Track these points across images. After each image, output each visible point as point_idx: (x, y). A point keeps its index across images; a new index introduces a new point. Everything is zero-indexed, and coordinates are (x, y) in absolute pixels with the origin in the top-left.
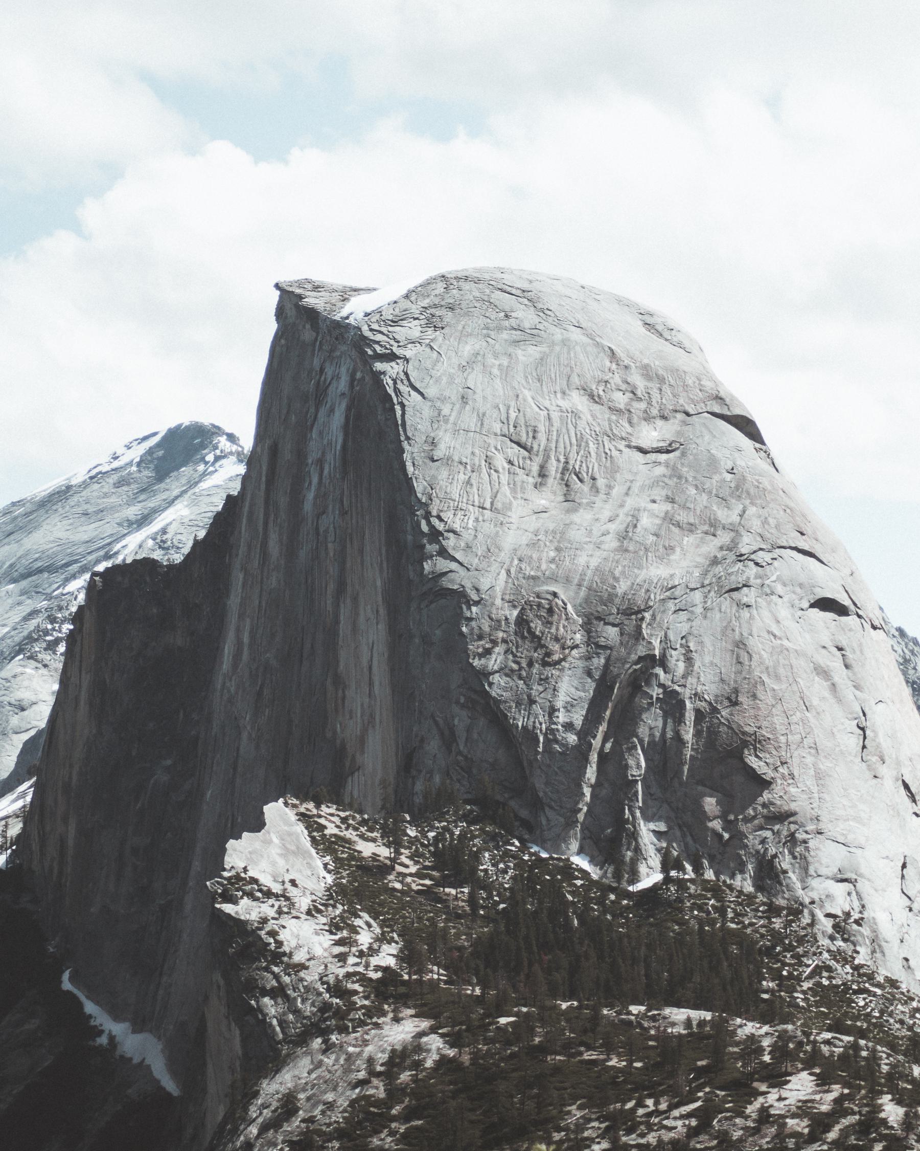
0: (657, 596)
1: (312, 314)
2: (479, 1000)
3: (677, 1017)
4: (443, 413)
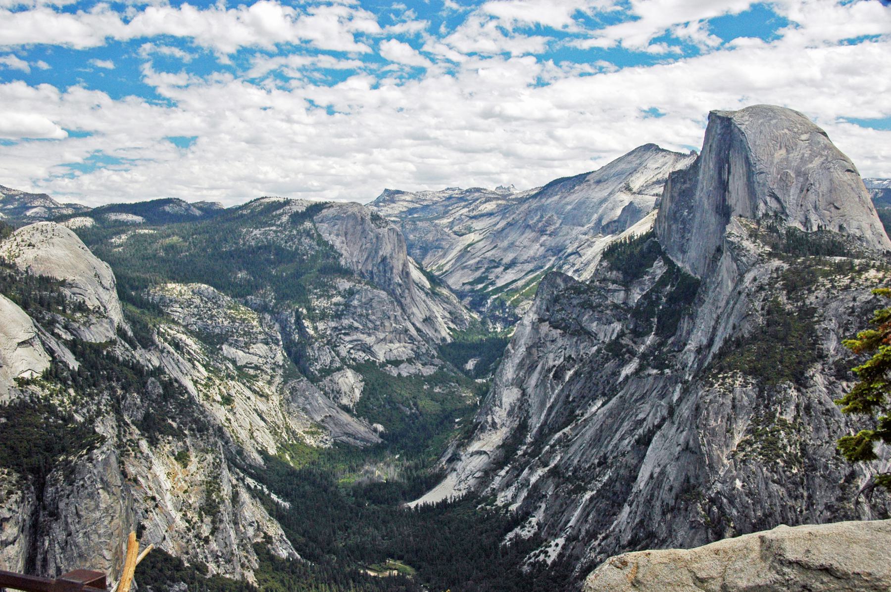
0: (811, 172)
1: (719, 117)
2: (792, 256)
3: (838, 259)
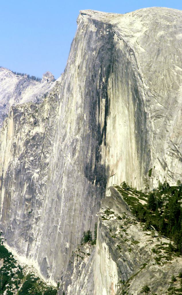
4: (152, 56)
